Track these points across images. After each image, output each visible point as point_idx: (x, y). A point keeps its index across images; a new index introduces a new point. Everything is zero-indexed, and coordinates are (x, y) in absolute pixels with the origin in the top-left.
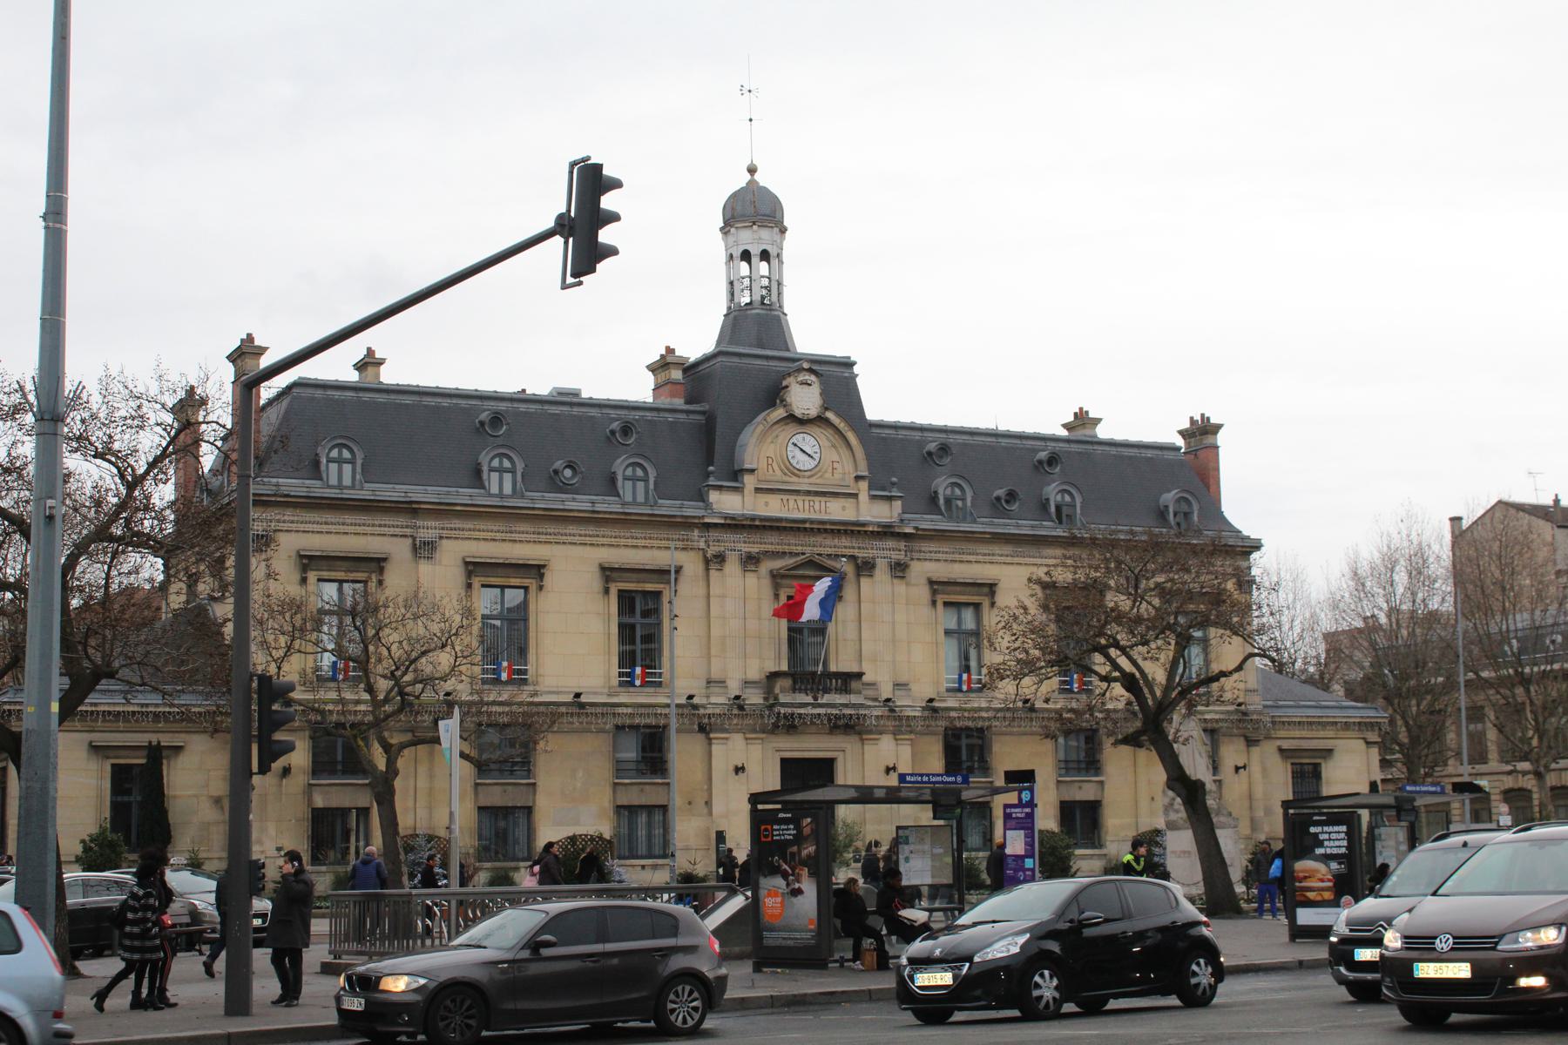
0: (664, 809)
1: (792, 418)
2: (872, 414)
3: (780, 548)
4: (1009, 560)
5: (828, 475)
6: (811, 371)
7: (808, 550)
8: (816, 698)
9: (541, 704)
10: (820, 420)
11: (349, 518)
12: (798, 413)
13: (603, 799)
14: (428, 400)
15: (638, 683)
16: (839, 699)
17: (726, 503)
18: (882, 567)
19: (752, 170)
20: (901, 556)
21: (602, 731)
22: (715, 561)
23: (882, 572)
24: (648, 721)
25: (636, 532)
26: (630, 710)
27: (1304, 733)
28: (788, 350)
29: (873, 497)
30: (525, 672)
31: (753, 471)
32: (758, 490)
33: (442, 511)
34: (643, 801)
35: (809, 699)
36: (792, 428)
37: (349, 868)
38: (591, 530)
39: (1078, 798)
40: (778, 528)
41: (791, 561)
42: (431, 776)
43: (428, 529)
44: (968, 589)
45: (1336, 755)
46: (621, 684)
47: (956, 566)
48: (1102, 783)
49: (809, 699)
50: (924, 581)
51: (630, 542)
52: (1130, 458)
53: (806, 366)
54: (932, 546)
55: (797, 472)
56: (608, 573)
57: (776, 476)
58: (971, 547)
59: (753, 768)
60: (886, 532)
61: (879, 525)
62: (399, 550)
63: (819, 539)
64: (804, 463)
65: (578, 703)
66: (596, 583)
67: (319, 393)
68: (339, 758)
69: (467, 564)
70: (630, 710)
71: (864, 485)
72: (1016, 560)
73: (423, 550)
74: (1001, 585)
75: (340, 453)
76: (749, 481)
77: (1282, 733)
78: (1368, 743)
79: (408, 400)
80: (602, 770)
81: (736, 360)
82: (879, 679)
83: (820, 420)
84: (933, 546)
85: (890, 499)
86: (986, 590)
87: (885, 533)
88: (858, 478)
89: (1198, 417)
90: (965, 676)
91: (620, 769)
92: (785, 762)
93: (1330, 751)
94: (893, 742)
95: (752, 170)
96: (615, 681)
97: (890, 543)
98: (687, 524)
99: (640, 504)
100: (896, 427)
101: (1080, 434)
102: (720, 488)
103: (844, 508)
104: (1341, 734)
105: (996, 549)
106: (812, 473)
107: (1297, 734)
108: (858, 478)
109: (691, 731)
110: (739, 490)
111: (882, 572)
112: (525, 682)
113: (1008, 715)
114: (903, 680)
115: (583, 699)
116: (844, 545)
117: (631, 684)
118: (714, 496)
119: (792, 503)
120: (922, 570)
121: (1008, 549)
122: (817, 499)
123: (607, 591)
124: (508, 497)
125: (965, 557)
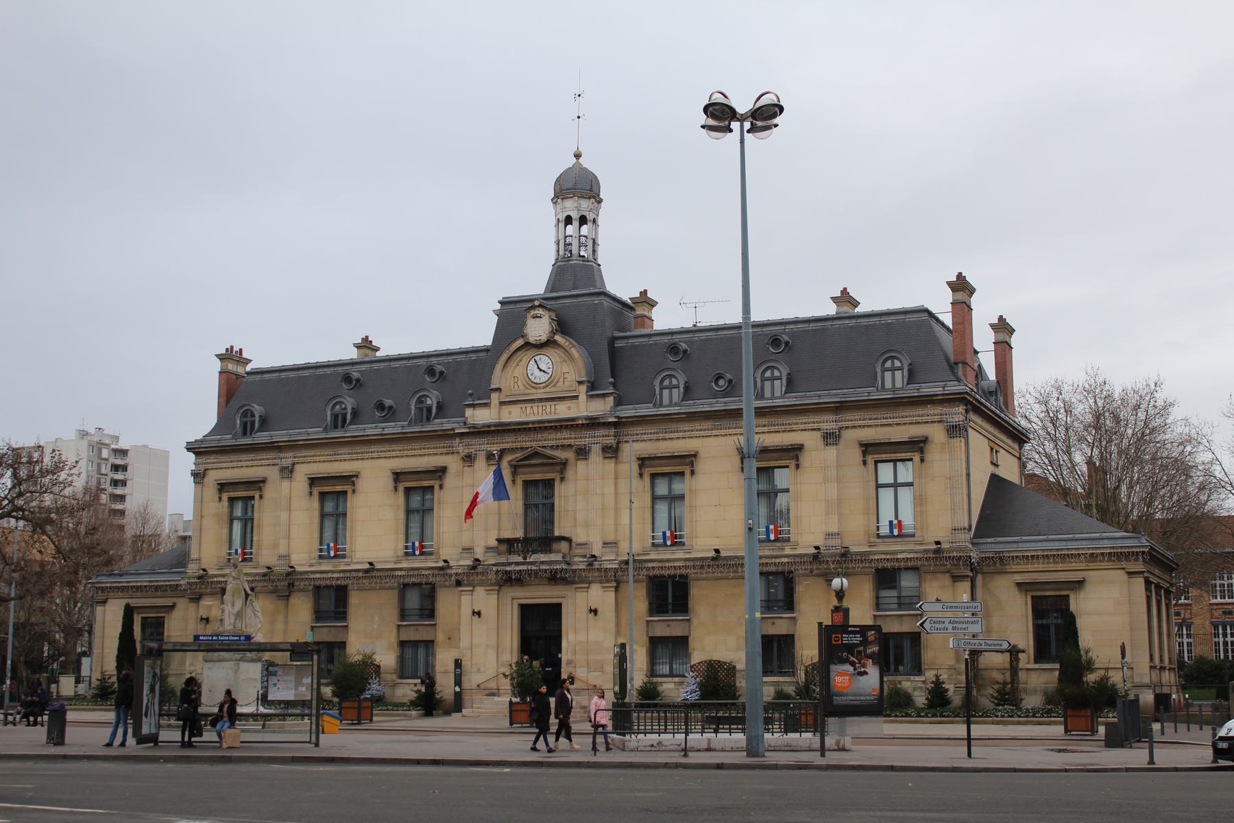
0: (429, 644)
1: (528, 345)
2: (488, 341)
3: (514, 445)
4: (709, 433)
5: (560, 384)
6: (540, 306)
7: (534, 444)
8: (525, 558)
9: (351, 571)
10: (549, 343)
11: (244, 457)
12: (532, 340)
13: (391, 637)
14: (320, 371)
15: (417, 553)
16: (543, 557)
17: (481, 416)
18: (596, 451)
19: (578, 156)
20: (611, 441)
21: (391, 588)
22: (469, 459)
23: (596, 455)
24: (328, 582)
25: (416, 445)
26: (403, 573)
27: (1052, 567)
28: (595, 286)
29: (591, 396)
30: (344, 550)
31: (499, 390)
32: (502, 403)
33: (293, 446)
34: (418, 637)
35: (520, 559)
36: (531, 352)
37: (801, 676)
38: (387, 447)
39: (770, 632)
40: (509, 431)
41: (519, 455)
42: (286, 622)
43: (287, 459)
44: (672, 461)
45: (1088, 586)
46: (406, 554)
47: (661, 443)
48: (794, 618)
49: (520, 559)
50: (634, 459)
51: (409, 453)
52: (868, 326)
53: (537, 303)
54: (638, 430)
55: (535, 385)
56: (398, 476)
57: (521, 389)
58: (674, 426)
59: (466, 611)
60: (593, 423)
61: (588, 418)
62: (272, 473)
63: (545, 435)
64: (541, 378)
65: (371, 569)
66: (391, 484)
67: (292, 374)
68: (670, 600)
69: (862, 445)
70: (403, 573)
71: (583, 388)
72: (715, 432)
73: (287, 472)
74: (701, 454)
75: (772, 373)
76: (495, 397)
77: (1015, 568)
78: (1129, 573)
79: (306, 373)
80: (392, 614)
81: (512, 306)
82: (591, 540)
83: (549, 343)
84: (638, 430)
85: (604, 396)
86: (558, 468)
87: (473, 433)
88: (580, 383)
89: (236, 349)
90: (772, 527)
91: (403, 615)
92: (524, 609)
93: (1080, 584)
94: (600, 591)
95: (578, 156)
96: (401, 552)
97: (602, 432)
98: (448, 435)
99: (676, 405)
100: (796, 322)
101: (846, 309)
102: (473, 406)
103: (569, 408)
104: (1092, 565)
105: (698, 426)
106: (547, 384)
107: (1030, 567)
108: (580, 383)
109: (450, 586)
110: (487, 405)
111: (596, 455)
112: (344, 556)
113: (699, 563)
114: (611, 538)
115: (378, 566)
116: (565, 437)
117: (414, 554)
118: (469, 412)
119: (535, 409)
120: (632, 449)
121: (708, 424)
122: (548, 404)
123: (396, 489)
124: (899, 389)
125: (668, 435)
